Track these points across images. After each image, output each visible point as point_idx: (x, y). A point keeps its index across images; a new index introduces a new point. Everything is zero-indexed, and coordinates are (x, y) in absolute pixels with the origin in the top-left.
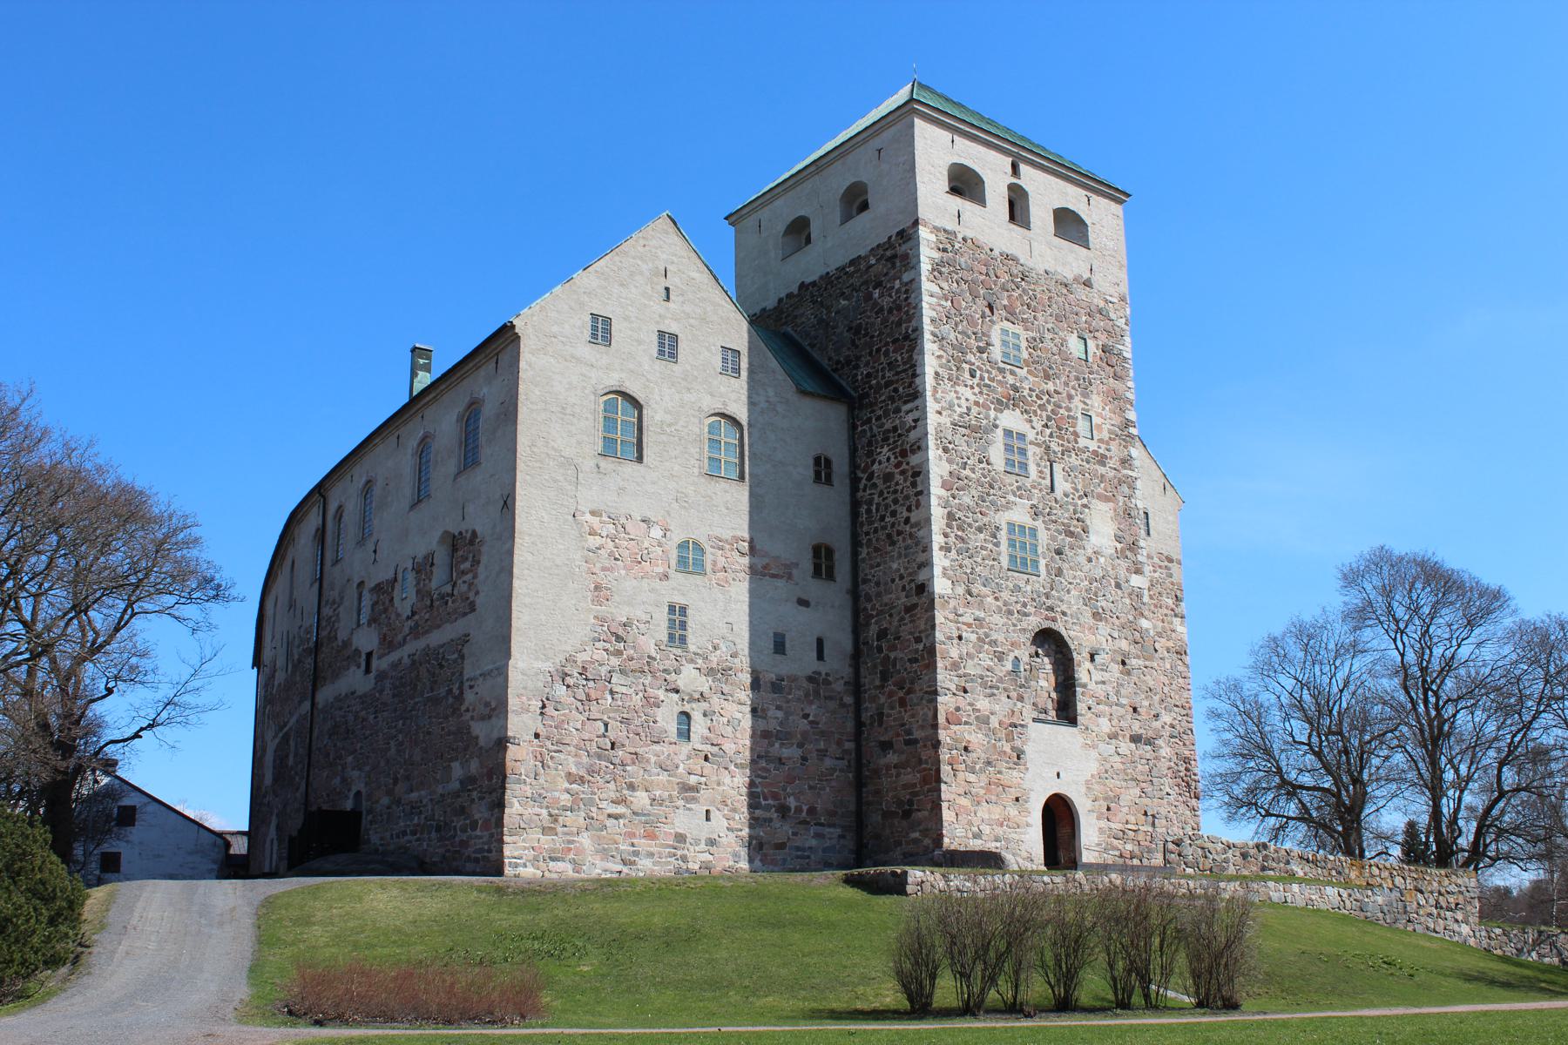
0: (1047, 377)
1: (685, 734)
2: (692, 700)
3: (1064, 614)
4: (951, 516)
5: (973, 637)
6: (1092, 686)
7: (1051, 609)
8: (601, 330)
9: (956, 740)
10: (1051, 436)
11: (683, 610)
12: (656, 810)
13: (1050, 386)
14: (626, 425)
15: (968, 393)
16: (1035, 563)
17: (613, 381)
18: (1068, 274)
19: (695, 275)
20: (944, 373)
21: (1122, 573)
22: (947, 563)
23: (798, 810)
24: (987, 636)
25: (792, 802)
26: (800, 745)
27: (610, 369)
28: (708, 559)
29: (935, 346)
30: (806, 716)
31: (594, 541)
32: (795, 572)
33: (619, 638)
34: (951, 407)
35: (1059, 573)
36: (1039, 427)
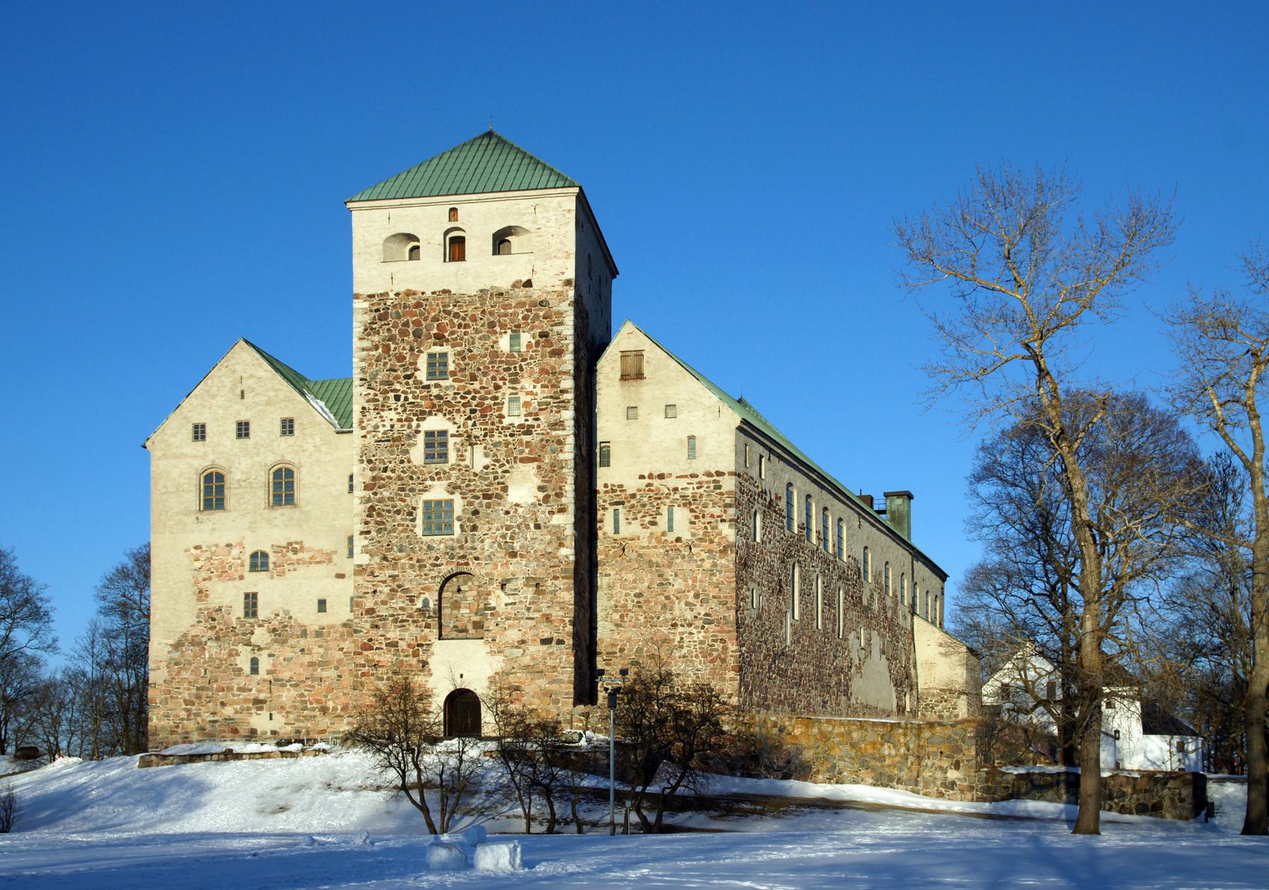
0: (473, 378)
1: (255, 670)
2: (260, 649)
3: (477, 559)
4: (372, 509)
5: (387, 590)
6: (501, 609)
7: (464, 557)
8: (199, 433)
9: (367, 661)
10: (474, 424)
11: (255, 595)
12: (238, 716)
13: (477, 385)
14: (214, 491)
15: (393, 415)
16: (450, 526)
17: (207, 463)
18: (505, 285)
19: (261, 373)
20: (371, 406)
21: (541, 518)
22: (366, 542)
23: (335, 709)
24: (399, 586)
25: (330, 704)
26: (336, 668)
27: (203, 457)
28: (272, 559)
29: (364, 390)
30: (341, 649)
31: (197, 565)
32: (334, 557)
33: (214, 619)
34: (376, 427)
35: (474, 528)
36: (460, 419)
